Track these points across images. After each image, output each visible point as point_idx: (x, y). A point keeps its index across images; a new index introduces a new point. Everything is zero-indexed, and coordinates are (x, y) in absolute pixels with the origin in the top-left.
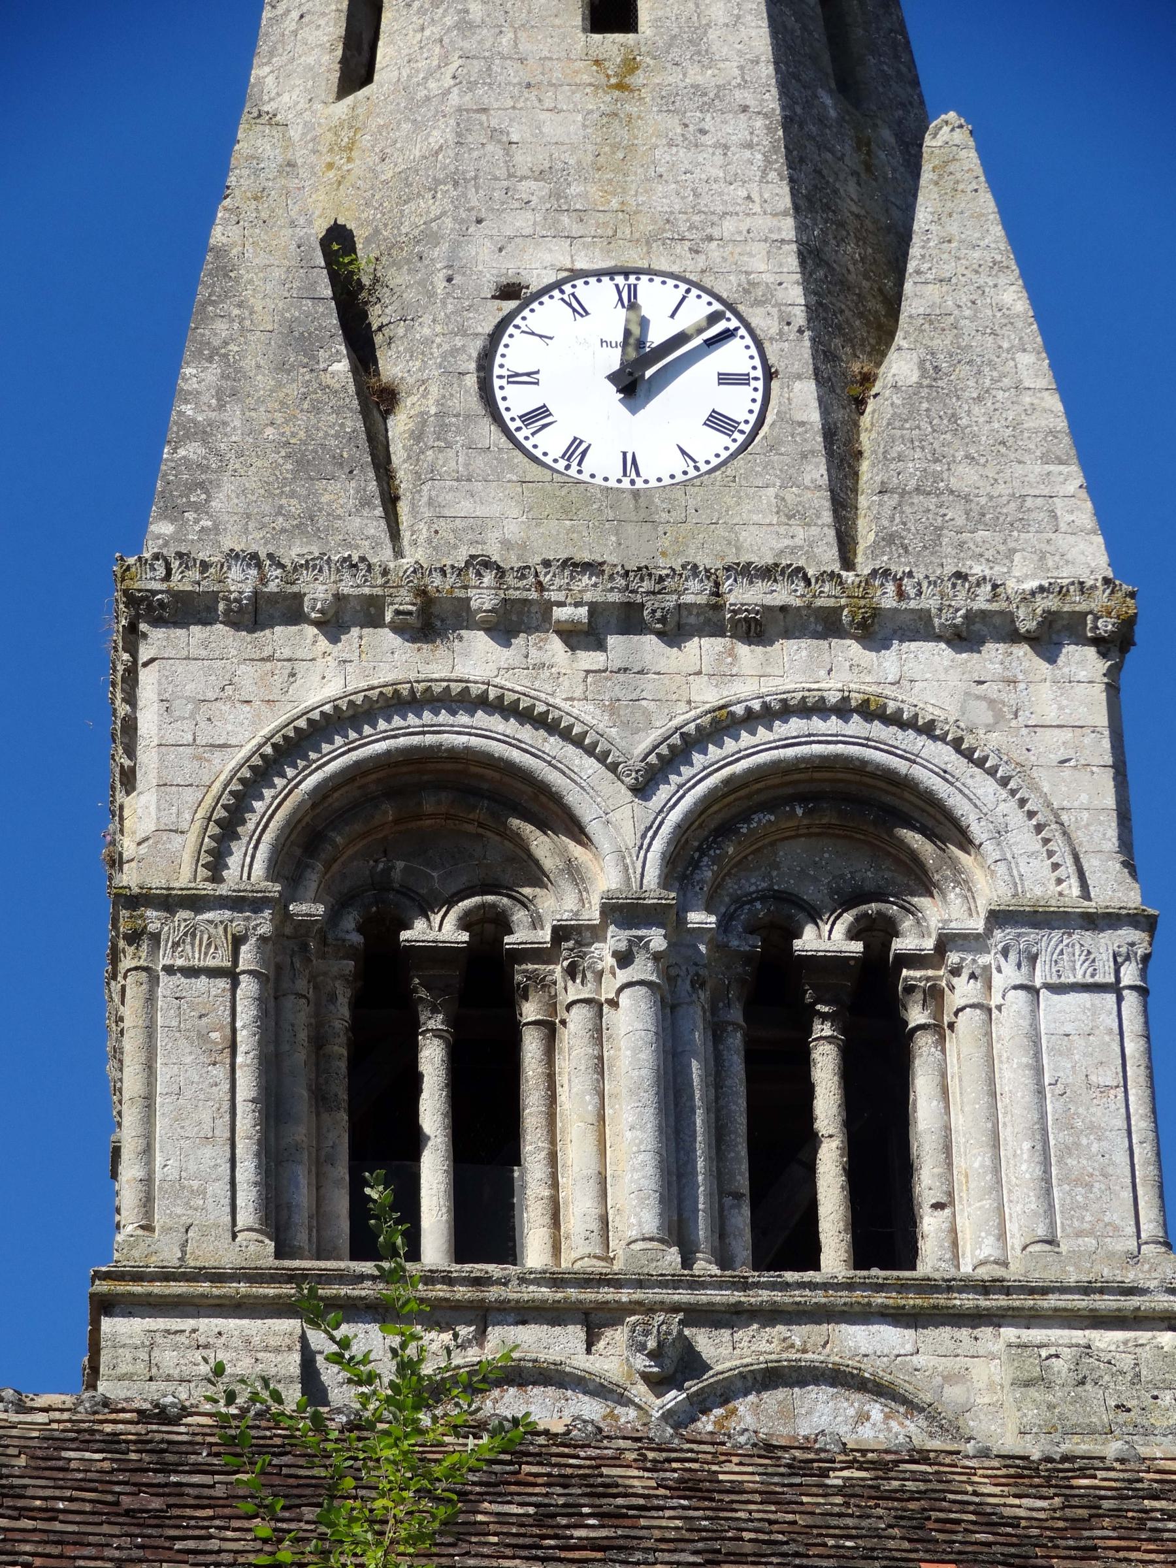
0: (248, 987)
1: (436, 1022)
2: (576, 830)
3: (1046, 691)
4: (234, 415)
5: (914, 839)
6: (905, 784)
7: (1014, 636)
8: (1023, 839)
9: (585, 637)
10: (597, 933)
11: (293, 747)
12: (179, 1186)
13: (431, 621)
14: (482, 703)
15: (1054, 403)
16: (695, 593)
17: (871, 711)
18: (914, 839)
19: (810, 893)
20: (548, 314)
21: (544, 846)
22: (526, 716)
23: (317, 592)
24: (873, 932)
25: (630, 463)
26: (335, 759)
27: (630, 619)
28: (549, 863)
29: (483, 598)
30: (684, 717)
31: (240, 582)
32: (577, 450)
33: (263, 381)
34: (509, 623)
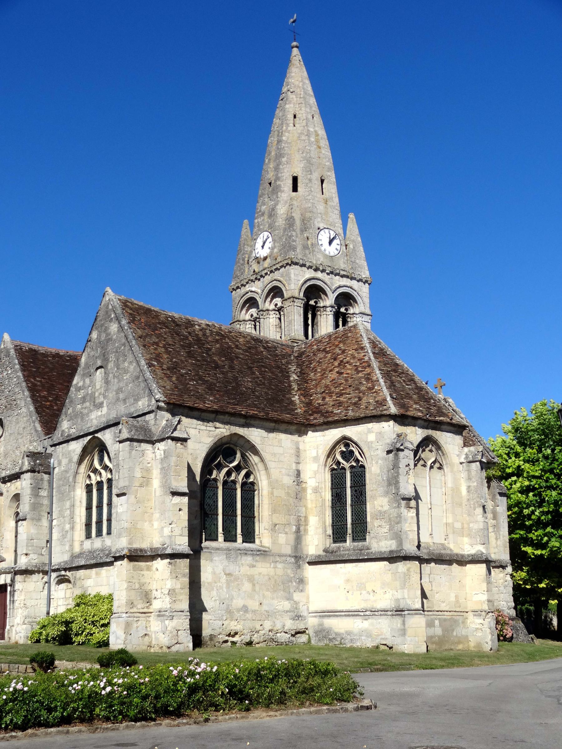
0: (302, 309)
1: (311, 312)
2: (326, 295)
3: (364, 288)
4: (297, 239)
5: (352, 301)
6: (353, 296)
7: (362, 281)
8: (362, 304)
9: (328, 274)
10: (328, 307)
11: (305, 282)
12: (297, 330)
13: (316, 270)
14: (320, 280)
15: (364, 253)
16: (338, 272)
17: (351, 288)
18: (352, 301)
19: (342, 304)
20: (322, 232)
21: (323, 296)
22: (324, 282)
23: (308, 264)
24: (346, 310)
25: (329, 253)
26: (309, 284)
27: (332, 273)
28: (323, 298)
29: (321, 269)
30: (337, 285)
31: (301, 262)
32: (325, 250)
33: (299, 235)
34: (323, 271)
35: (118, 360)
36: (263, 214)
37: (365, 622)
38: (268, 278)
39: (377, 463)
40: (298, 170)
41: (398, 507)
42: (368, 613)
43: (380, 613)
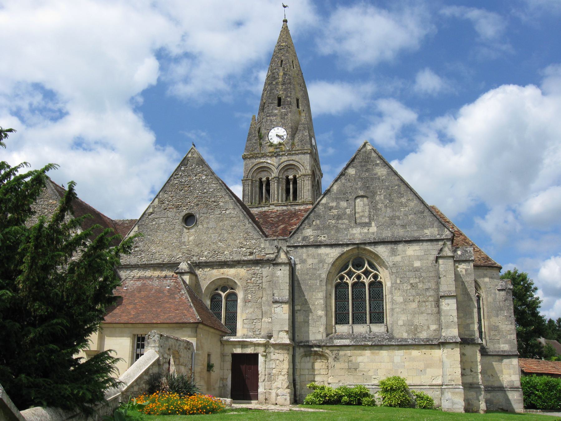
35: (390, 195)
36: (276, 115)
37: (488, 394)
38: (284, 158)
39: (491, 295)
40: (299, 95)
41: (511, 324)
42: (489, 389)
43: (497, 389)
